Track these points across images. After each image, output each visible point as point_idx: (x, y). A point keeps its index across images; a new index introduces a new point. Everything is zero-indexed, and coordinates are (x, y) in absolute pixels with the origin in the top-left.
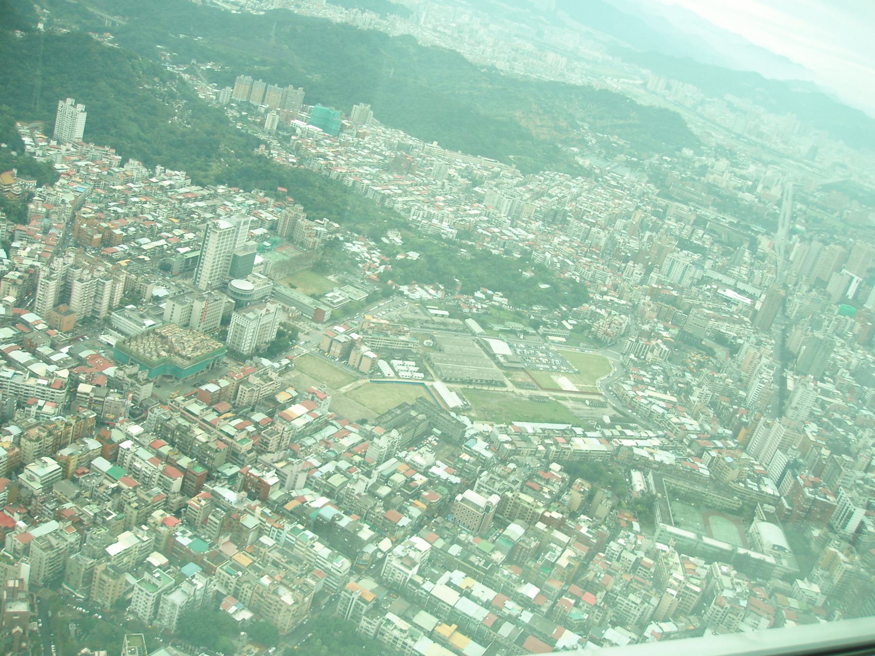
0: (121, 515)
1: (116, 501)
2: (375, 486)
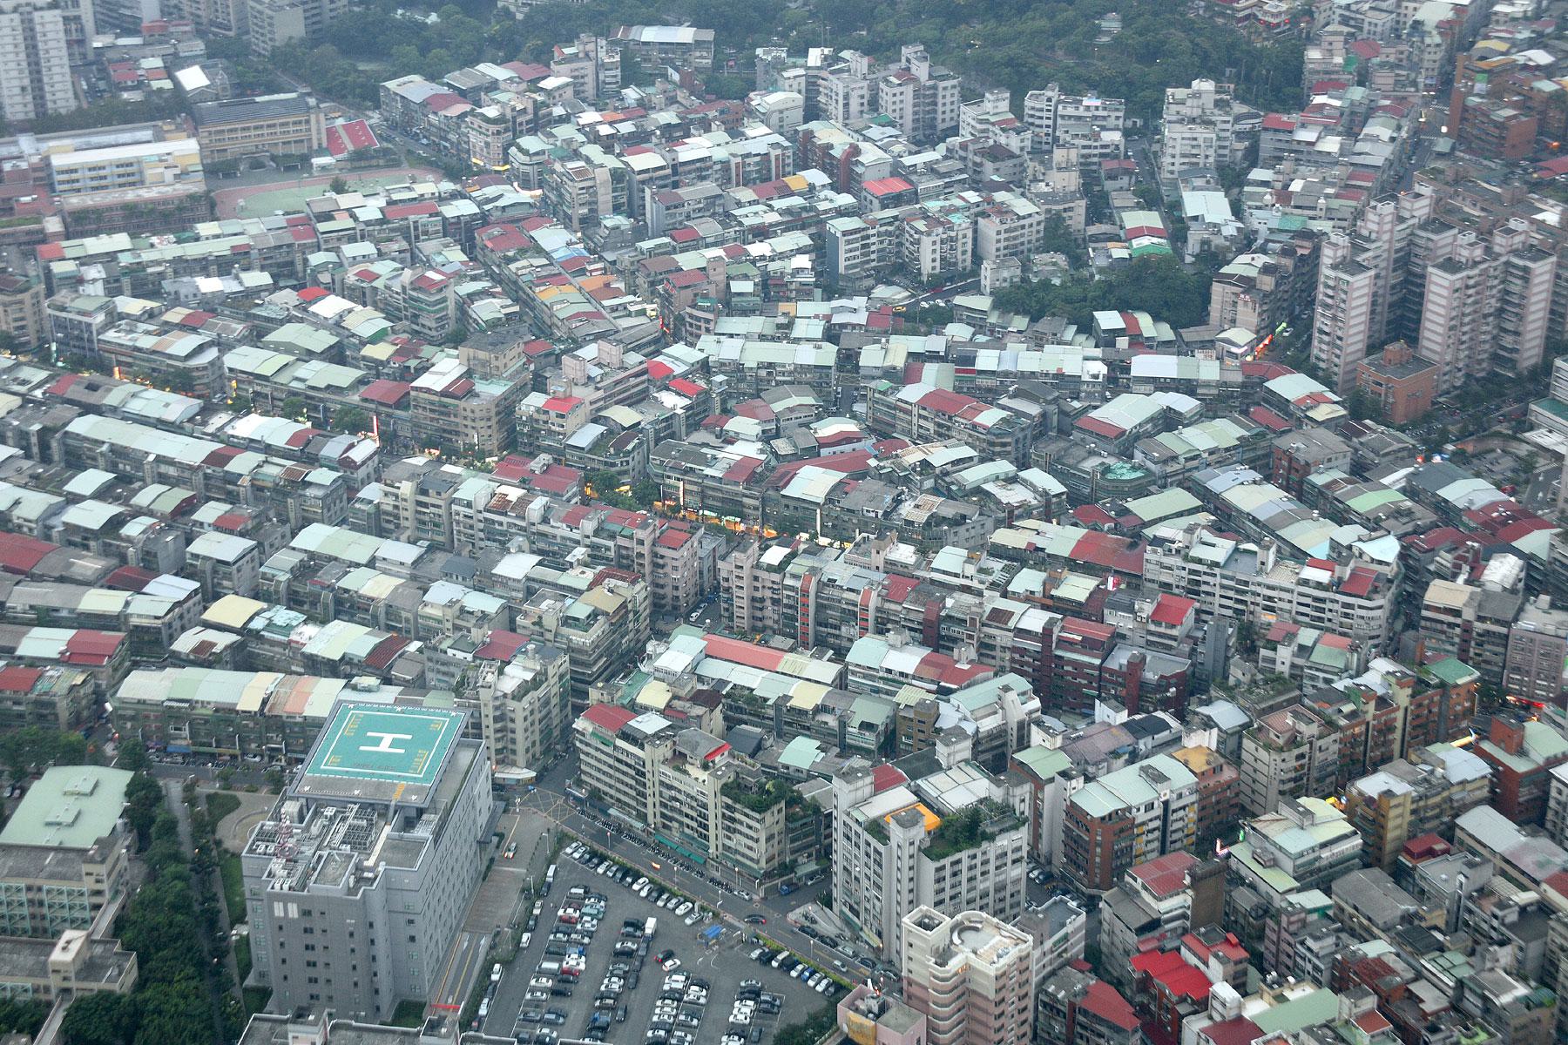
1: (1534, 949)
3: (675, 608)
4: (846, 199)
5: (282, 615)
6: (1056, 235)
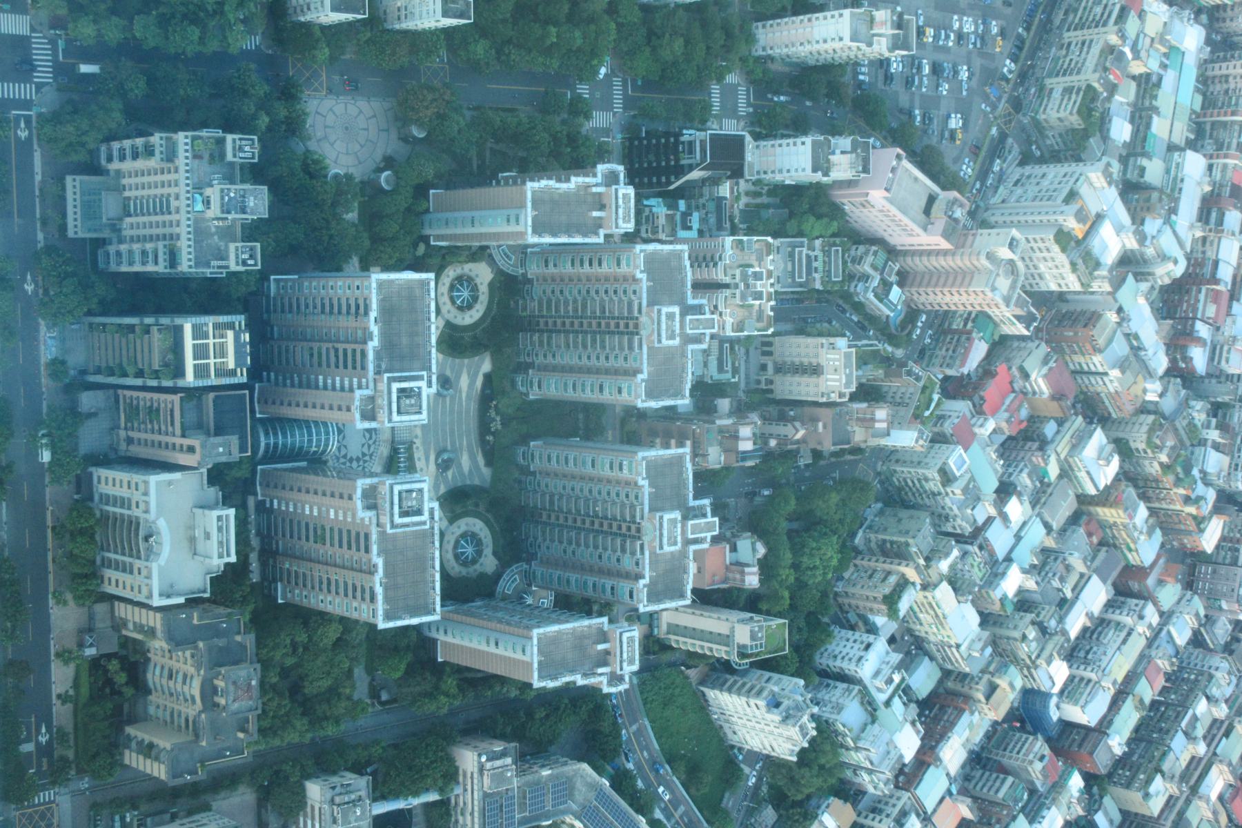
0: (1010, 609)
3: (1218, 19)
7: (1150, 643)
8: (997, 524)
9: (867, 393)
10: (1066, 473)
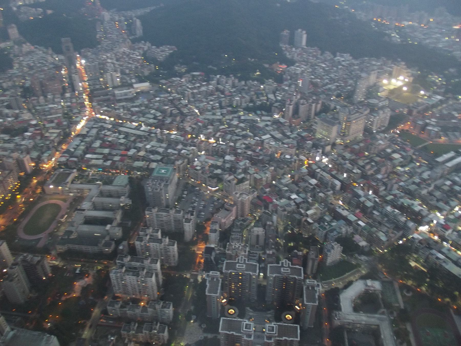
2: (432, 191)
4: (223, 96)
5: (148, 154)
6: (252, 101)
7: (324, 171)
8: (296, 201)
9: (264, 226)
10: (286, 186)
